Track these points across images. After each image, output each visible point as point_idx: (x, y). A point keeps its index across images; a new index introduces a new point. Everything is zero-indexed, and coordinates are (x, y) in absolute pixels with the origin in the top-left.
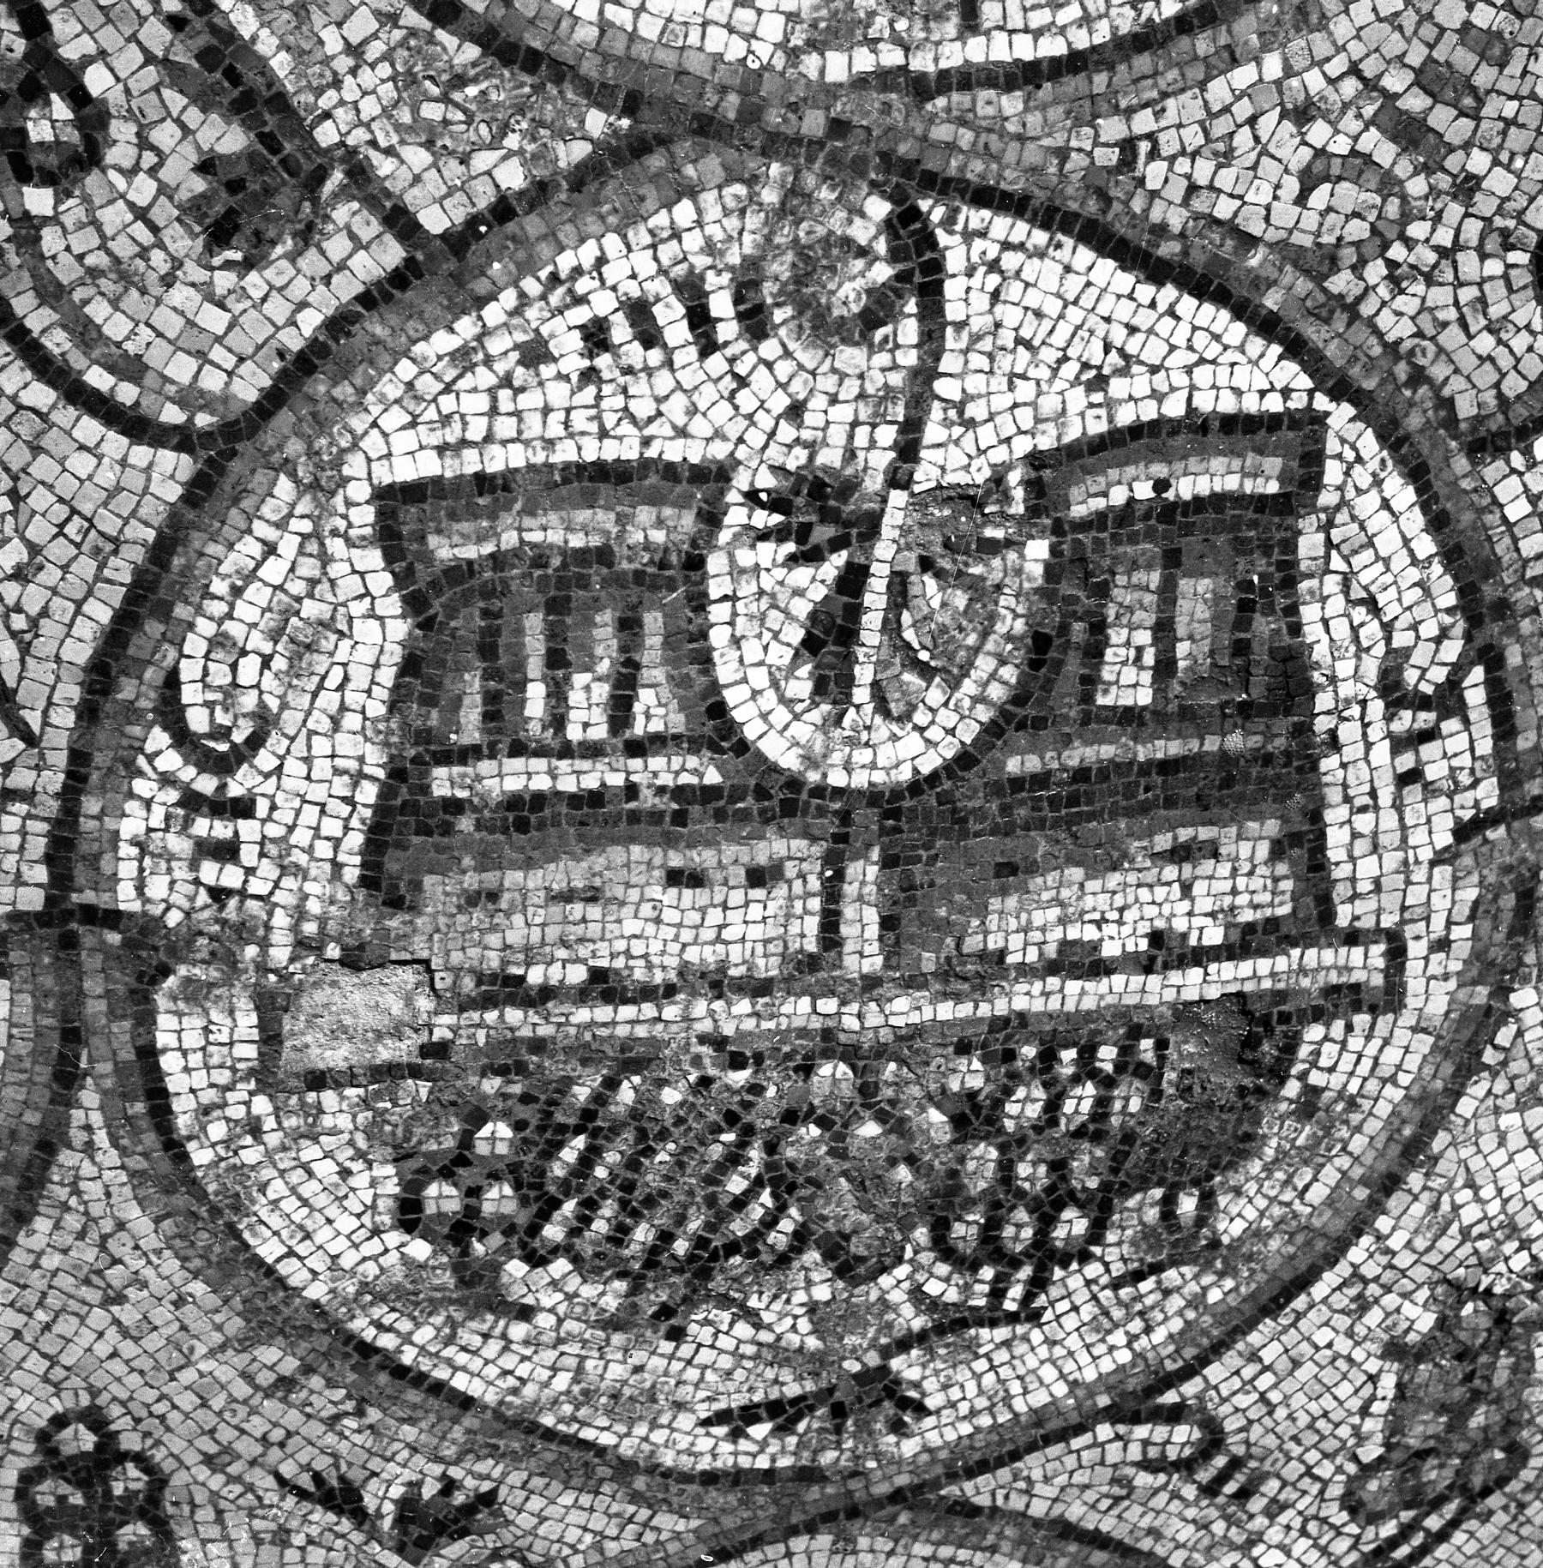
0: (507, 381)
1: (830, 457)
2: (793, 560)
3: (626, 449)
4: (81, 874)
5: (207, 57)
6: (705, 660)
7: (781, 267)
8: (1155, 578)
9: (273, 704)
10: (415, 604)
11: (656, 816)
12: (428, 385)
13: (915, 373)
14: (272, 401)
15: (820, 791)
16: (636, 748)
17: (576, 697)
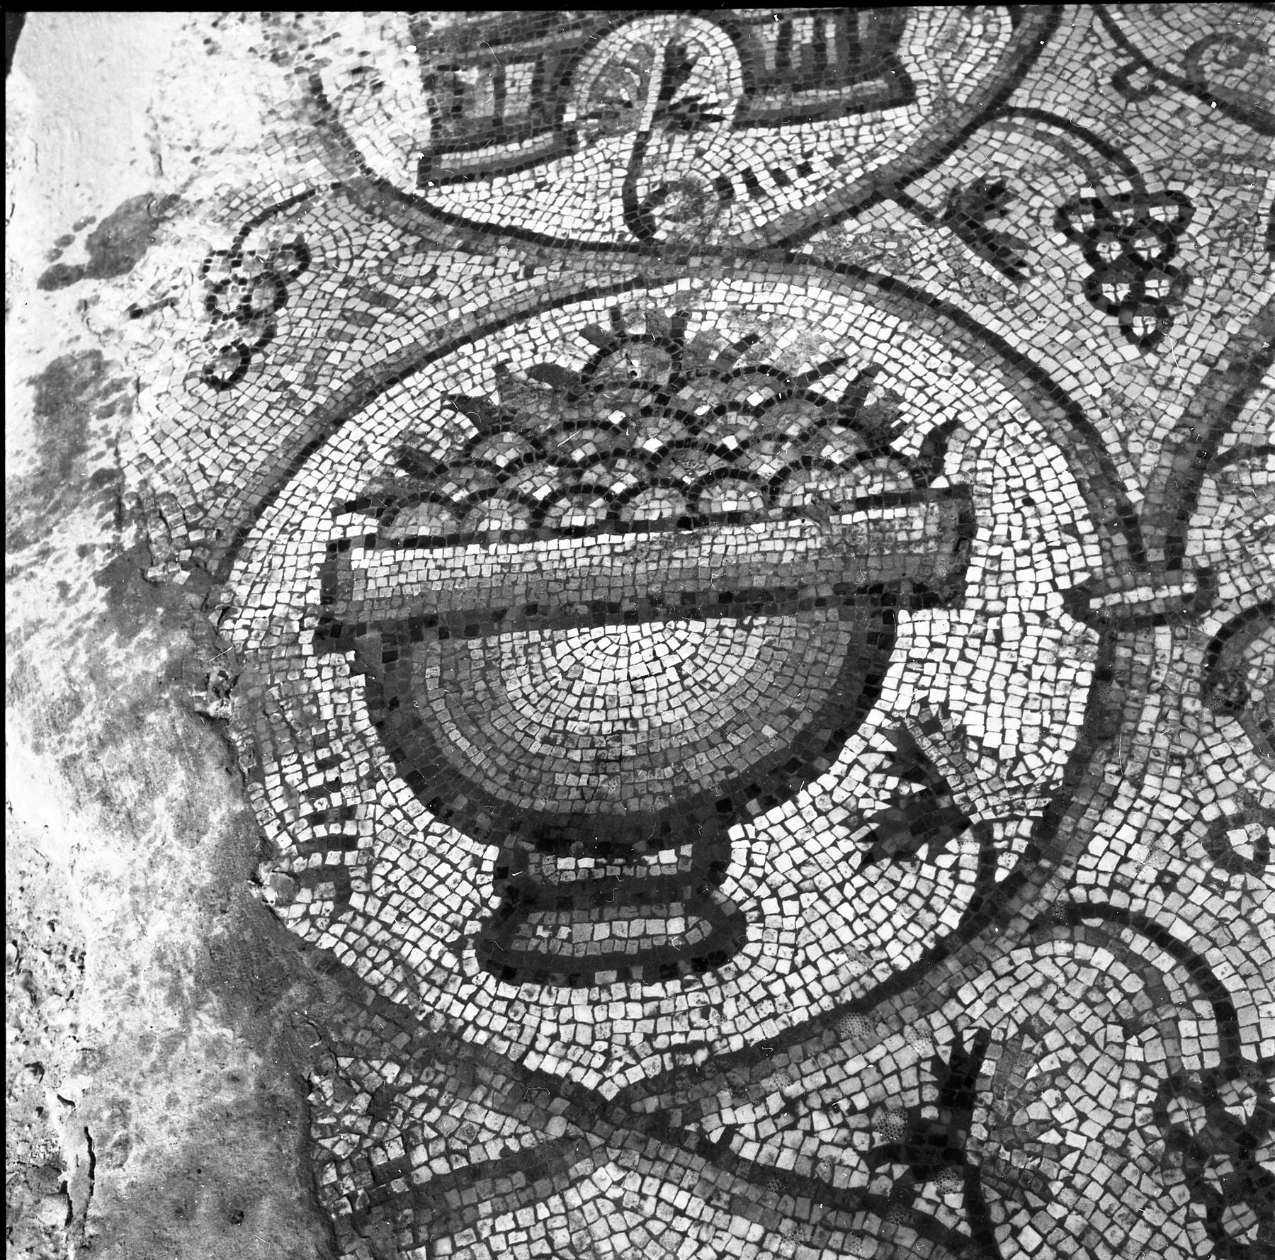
0: (850, 149)
1: (680, 139)
3: (785, 131)
6: (742, 55)
7: (709, 206)
8: (507, 113)
10: (895, 63)
12: (890, 144)
13: (639, 176)
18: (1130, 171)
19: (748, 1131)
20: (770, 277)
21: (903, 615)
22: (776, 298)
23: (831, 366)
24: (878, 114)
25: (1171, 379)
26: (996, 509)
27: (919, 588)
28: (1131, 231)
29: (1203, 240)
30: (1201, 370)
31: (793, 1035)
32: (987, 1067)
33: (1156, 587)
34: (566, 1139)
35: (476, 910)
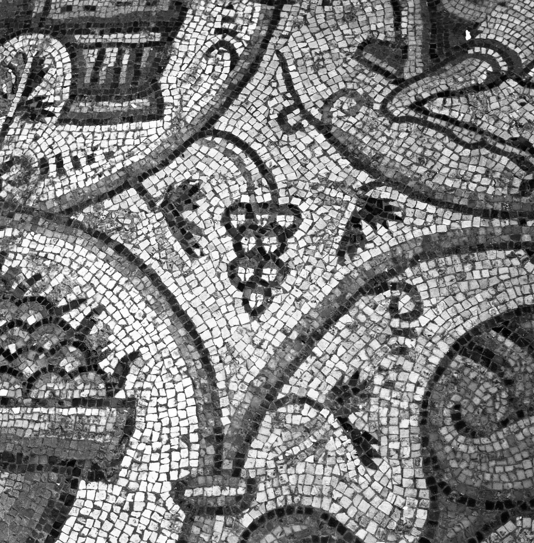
0: (119, 148)
1: (28, 126)
2: (44, 97)
4: (270, 14)
5: (190, 236)
6: (74, 69)
7: (34, 178)
9: (204, 60)
10: (157, 87)
11: (96, 26)
12: (142, 147)
14: (188, 143)
15: (46, 33)
16: (98, 45)
17: (113, 60)
18: (273, 186)
21: (82, 484)
22: (57, 250)
23: (75, 304)
24: (140, 124)
25: (263, 341)
26: (148, 418)
27: (95, 466)
28: (263, 231)
29: (302, 243)
30: (281, 337)
33: (223, 488)
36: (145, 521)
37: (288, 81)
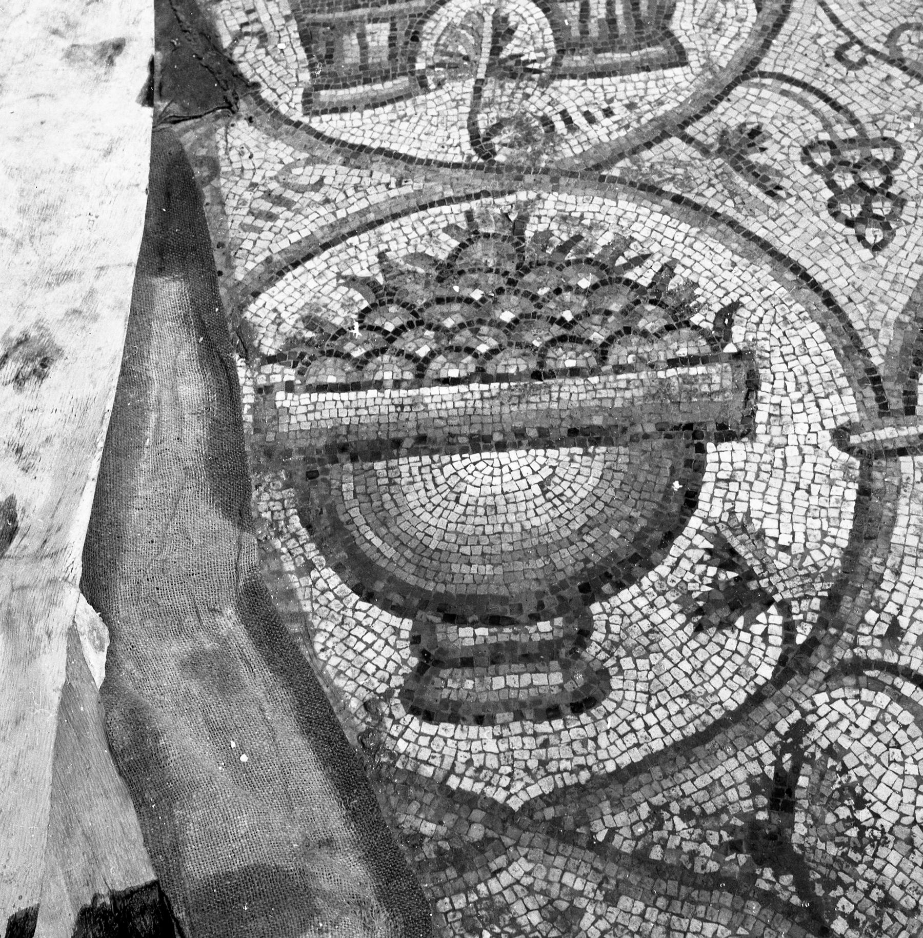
1: (510, 85)
2: (521, 55)
5: (766, 179)
6: (553, 24)
8: (370, 61)
10: (670, 34)
12: (673, 95)
14: (730, 87)
18: (854, 121)
19: (626, 832)
20: (588, 191)
21: (710, 447)
23: (640, 260)
24: (660, 72)
26: (774, 368)
27: (722, 426)
31: (653, 759)
32: (803, 781)
34: (487, 840)
35: (399, 667)
36: (807, 475)
37: (834, 19)
